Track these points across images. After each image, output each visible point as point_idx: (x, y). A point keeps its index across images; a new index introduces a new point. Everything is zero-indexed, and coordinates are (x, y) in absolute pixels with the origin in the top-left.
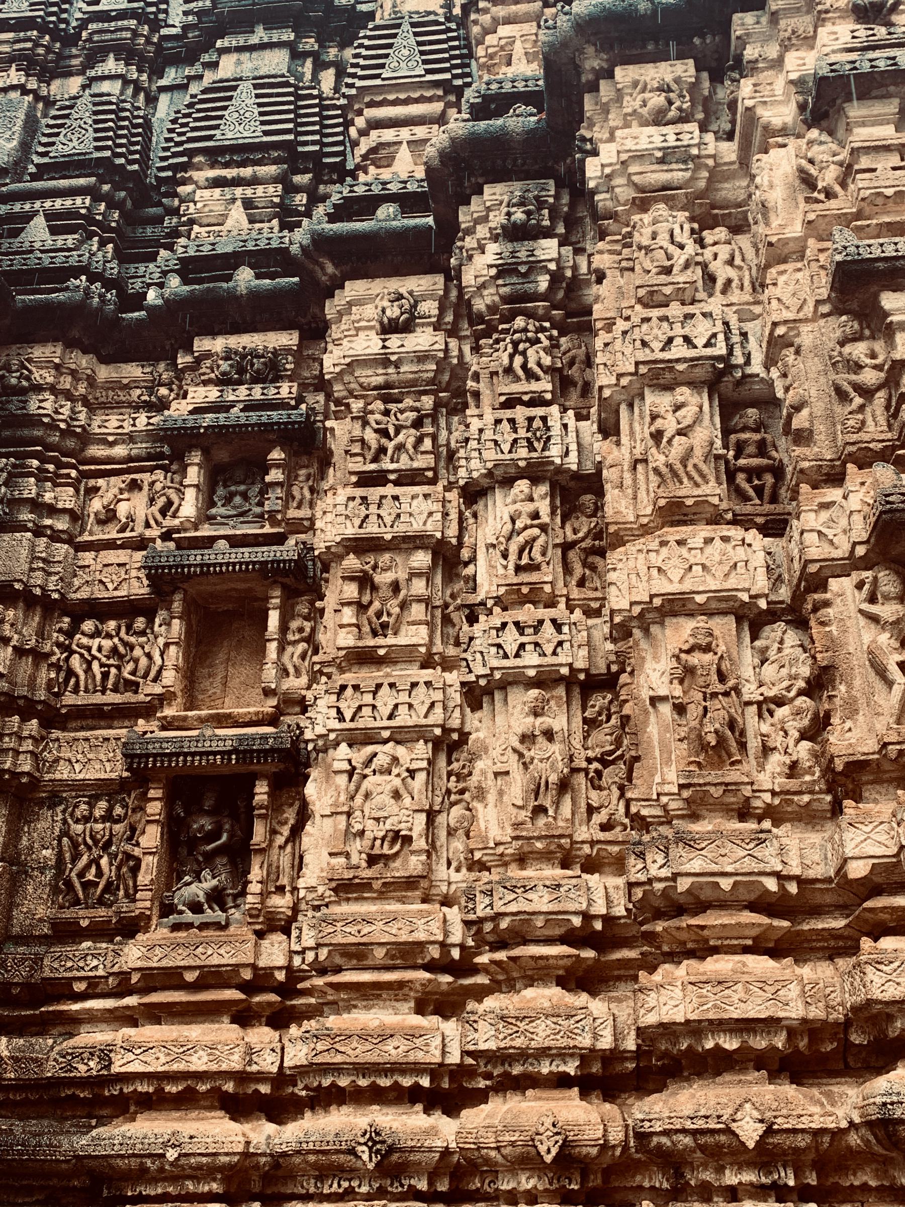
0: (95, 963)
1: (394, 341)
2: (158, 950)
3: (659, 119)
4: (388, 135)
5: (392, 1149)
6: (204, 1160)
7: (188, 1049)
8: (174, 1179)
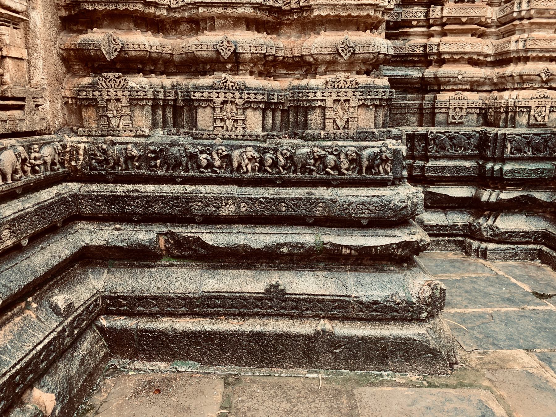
0: (420, 14)
2: (453, 10)
5: (551, 75)
6: (469, 79)
7: (464, 44)
8: (455, 84)
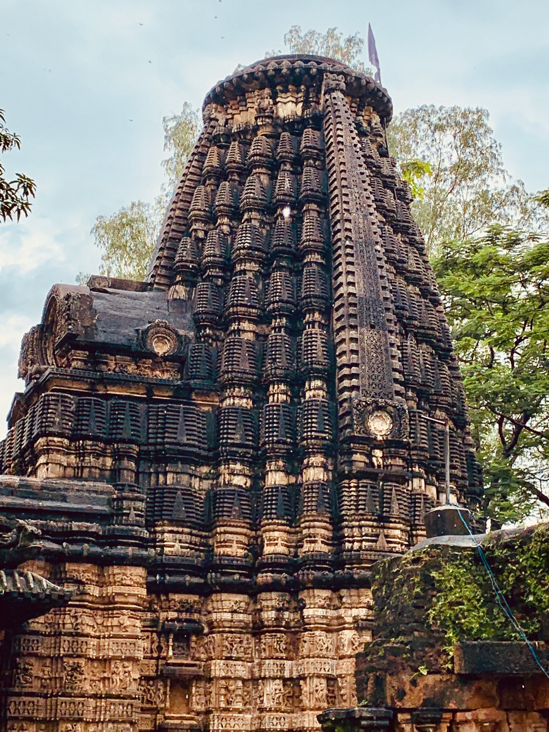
1: (235, 615)
3: (322, 607)
4: (230, 536)
